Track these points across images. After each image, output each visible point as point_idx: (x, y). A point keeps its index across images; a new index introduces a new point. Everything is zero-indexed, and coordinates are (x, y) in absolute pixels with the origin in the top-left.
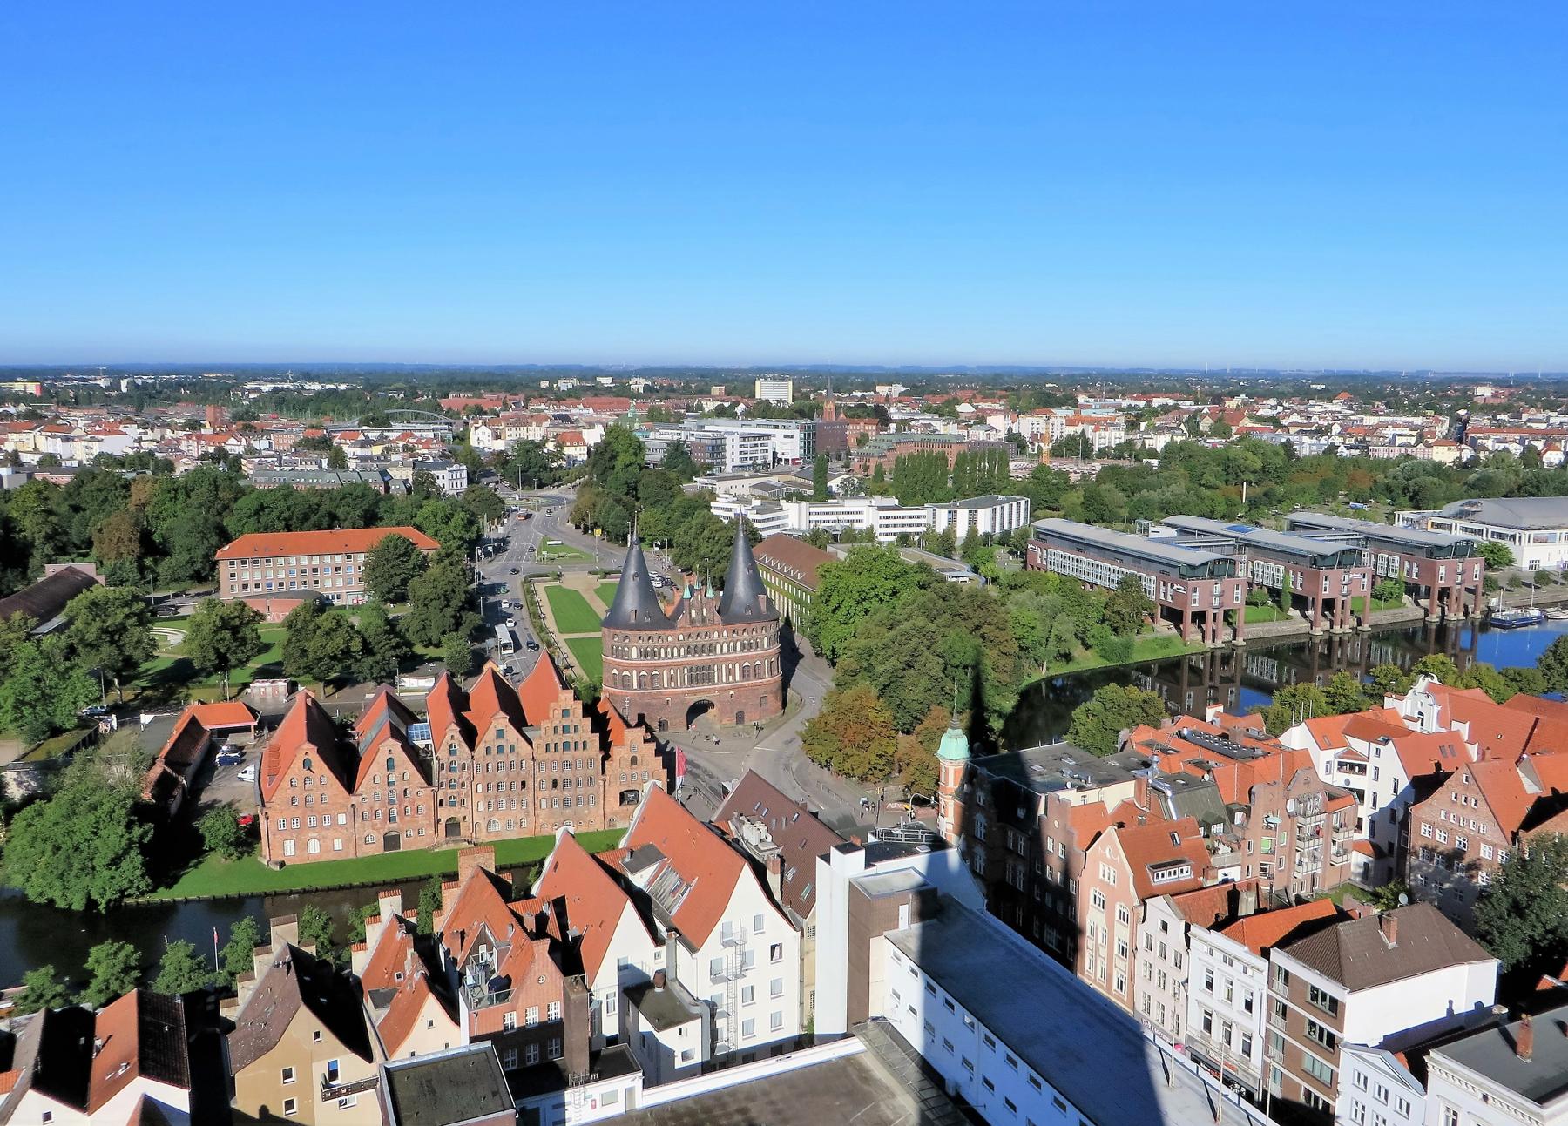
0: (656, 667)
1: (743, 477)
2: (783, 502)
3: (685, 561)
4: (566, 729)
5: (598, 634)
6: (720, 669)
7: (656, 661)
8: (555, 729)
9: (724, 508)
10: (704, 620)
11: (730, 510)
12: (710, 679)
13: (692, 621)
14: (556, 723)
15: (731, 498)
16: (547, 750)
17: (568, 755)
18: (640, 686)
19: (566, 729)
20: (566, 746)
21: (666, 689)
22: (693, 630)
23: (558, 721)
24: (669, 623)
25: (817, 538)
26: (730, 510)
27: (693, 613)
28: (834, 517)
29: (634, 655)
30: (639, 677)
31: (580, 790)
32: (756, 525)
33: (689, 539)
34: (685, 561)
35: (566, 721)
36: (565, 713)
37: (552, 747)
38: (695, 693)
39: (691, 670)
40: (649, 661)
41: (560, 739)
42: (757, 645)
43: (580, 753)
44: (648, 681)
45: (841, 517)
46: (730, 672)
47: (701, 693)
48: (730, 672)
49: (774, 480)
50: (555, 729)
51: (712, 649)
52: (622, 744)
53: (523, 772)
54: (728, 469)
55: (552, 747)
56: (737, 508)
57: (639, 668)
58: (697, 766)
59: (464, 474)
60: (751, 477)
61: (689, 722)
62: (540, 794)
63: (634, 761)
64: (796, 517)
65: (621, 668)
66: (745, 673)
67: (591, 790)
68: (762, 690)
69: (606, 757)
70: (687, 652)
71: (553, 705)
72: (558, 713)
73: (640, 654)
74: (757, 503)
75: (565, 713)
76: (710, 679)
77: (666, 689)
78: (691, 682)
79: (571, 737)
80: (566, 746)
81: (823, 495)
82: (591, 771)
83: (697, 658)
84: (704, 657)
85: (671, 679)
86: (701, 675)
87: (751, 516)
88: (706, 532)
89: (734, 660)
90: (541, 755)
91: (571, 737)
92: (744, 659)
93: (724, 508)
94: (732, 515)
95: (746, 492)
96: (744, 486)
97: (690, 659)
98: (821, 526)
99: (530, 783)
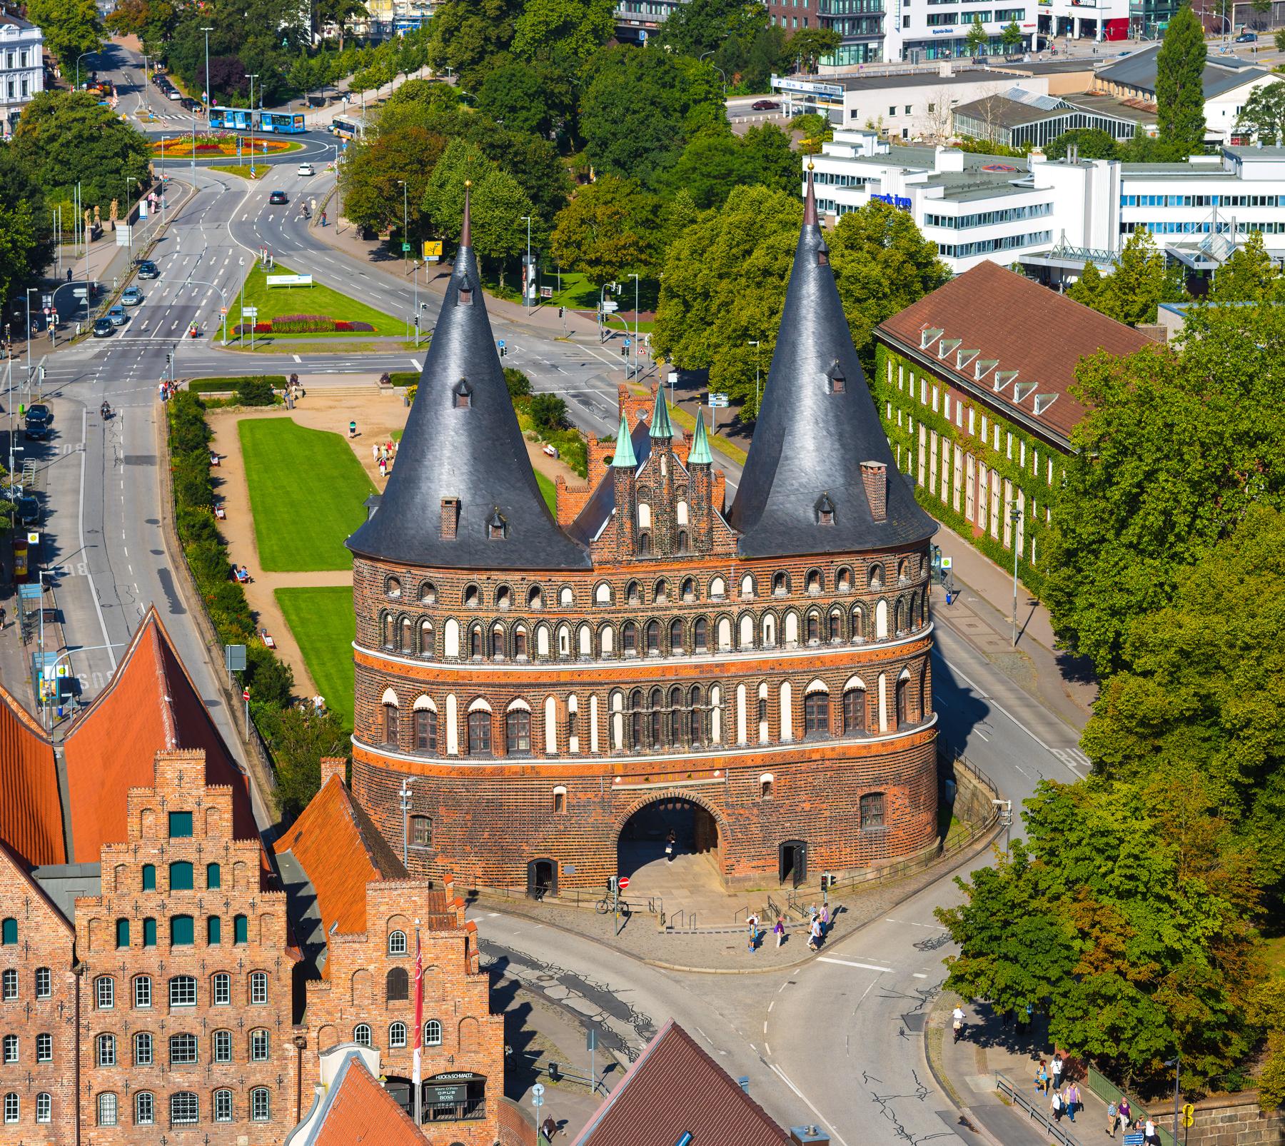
0: (520, 688)
1: (932, 78)
2: (1037, 158)
3: (695, 345)
4: (180, 874)
5: (344, 579)
6: (729, 702)
7: (520, 667)
8: (148, 870)
9: (848, 173)
10: (679, 538)
11: (857, 183)
12: (696, 731)
13: (642, 541)
14: (149, 853)
15: (870, 146)
16: (121, 938)
17: (186, 959)
18: (468, 748)
19: (180, 874)
20: (180, 928)
21: (552, 754)
22: (644, 573)
23: (155, 847)
24: (565, 548)
25: (1138, 283)
26: (857, 183)
27: (645, 516)
28: (1201, 214)
29: (452, 644)
30: (467, 717)
31: (224, 1073)
32: (932, 235)
33: (704, 273)
34: (695, 345)
35: (182, 849)
36: (180, 823)
37: (136, 929)
38: (647, 774)
39: (634, 698)
40: (497, 666)
41: (162, 903)
42: (854, 623)
43: (225, 954)
44: (502, 729)
45: (1227, 214)
46: (763, 710)
47: (670, 772)
48: (763, 710)
49: (1035, 90)
50: (148, 870)
51: (703, 633)
52: (355, 925)
53: (44, 1006)
54: (890, 50)
55: (136, 929)
56: (893, 182)
57: (466, 688)
58: (623, 1012)
59: (35, 56)
60: (962, 77)
61: (626, 868)
62: (99, 1077)
63: (397, 985)
64: (1075, 210)
65: (412, 685)
66: (813, 712)
67: (260, 1072)
68: (862, 778)
69: (306, 973)
70: (624, 642)
71: (138, 794)
72: (156, 822)
73: (472, 644)
74: (951, 162)
75: (180, 823)
76: (696, 731)
77: (552, 754)
78: (633, 738)
79: (196, 901)
80: (180, 928)
81: (1181, 140)
82: (259, 1013)
83: (654, 660)
84: (678, 658)
85: (570, 725)
86: (667, 715)
87: (926, 204)
88: (759, 257)
89: (777, 674)
90: (102, 954)
91: (196, 901)
92: (813, 668)
93: (848, 173)
94: (859, 199)
95: (918, 126)
96: (917, 110)
97: (633, 662)
98: (1161, 242)
99: (65, 1037)
